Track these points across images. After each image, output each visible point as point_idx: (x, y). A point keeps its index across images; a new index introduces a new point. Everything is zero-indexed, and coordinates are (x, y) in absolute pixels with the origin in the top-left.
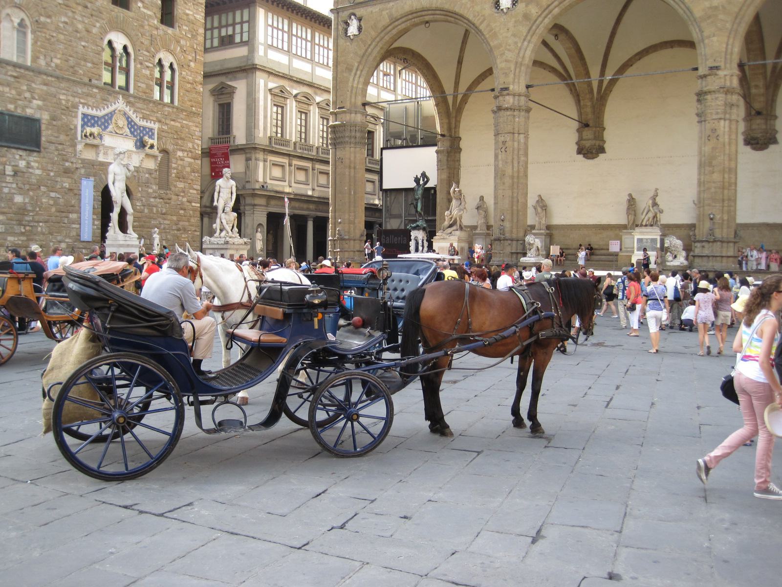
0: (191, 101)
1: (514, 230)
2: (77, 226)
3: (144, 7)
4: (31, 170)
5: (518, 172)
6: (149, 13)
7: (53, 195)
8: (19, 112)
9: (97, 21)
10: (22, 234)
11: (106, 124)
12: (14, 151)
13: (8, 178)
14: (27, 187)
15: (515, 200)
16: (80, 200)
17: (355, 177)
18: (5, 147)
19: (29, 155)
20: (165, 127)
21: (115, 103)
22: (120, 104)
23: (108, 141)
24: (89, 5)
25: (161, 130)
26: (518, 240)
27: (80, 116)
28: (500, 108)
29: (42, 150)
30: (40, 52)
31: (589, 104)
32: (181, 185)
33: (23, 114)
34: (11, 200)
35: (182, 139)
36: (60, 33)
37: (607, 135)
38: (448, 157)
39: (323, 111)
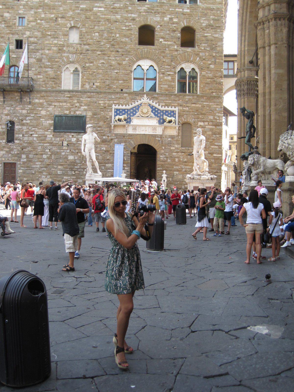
0: (211, 89)
2: (112, 171)
3: (165, 41)
6: (169, 43)
8: (72, 113)
9: (127, 57)
10: (74, 175)
11: (134, 113)
13: (64, 147)
14: (77, 151)
16: (113, 156)
18: (63, 132)
21: (140, 100)
22: (145, 100)
23: (135, 121)
24: (120, 50)
30: (86, 82)
33: (75, 115)
34: (67, 158)
35: (202, 114)
36: (99, 69)
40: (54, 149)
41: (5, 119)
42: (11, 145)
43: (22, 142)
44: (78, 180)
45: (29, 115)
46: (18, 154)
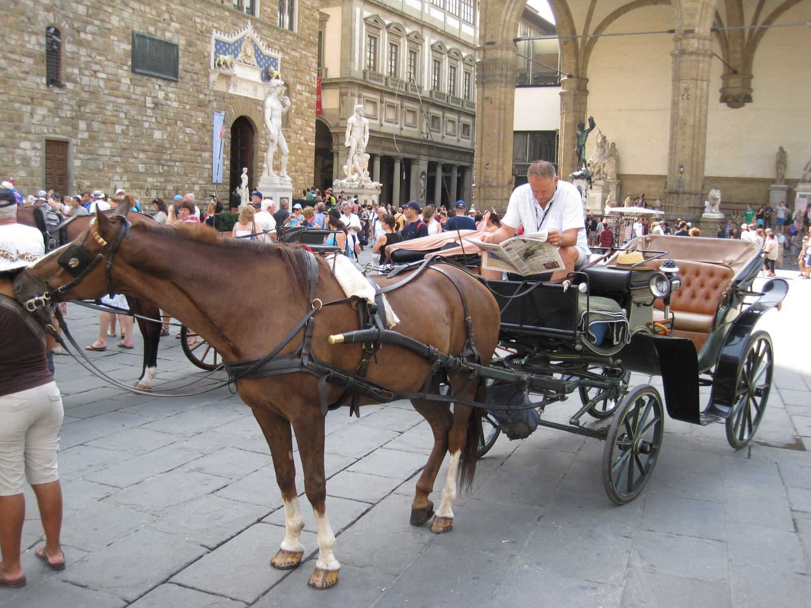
0: (309, 29)
1: (693, 184)
2: (209, 166)
4: (169, 103)
5: (700, 121)
7: (188, 130)
8: (159, 36)
10: (160, 174)
11: (236, 52)
12: (154, 80)
13: (149, 111)
14: (165, 121)
15: (695, 151)
17: (505, 119)
18: (146, 75)
19: (168, 86)
20: (287, 57)
22: (248, 31)
25: (283, 61)
26: (696, 194)
27: (213, 42)
28: (683, 52)
29: (179, 79)
31: (739, 49)
32: (299, 122)
33: (162, 39)
34: (151, 135)
35: (302, 71)
37: (754, 83)
38: (575, 100)
39: (412, 44)
40: (133, 112)
41: (45, 18)
42: (57, 94)
43: (78, 88)
44: (168, 184)
45: (90, 19)
46: (72, 118)
